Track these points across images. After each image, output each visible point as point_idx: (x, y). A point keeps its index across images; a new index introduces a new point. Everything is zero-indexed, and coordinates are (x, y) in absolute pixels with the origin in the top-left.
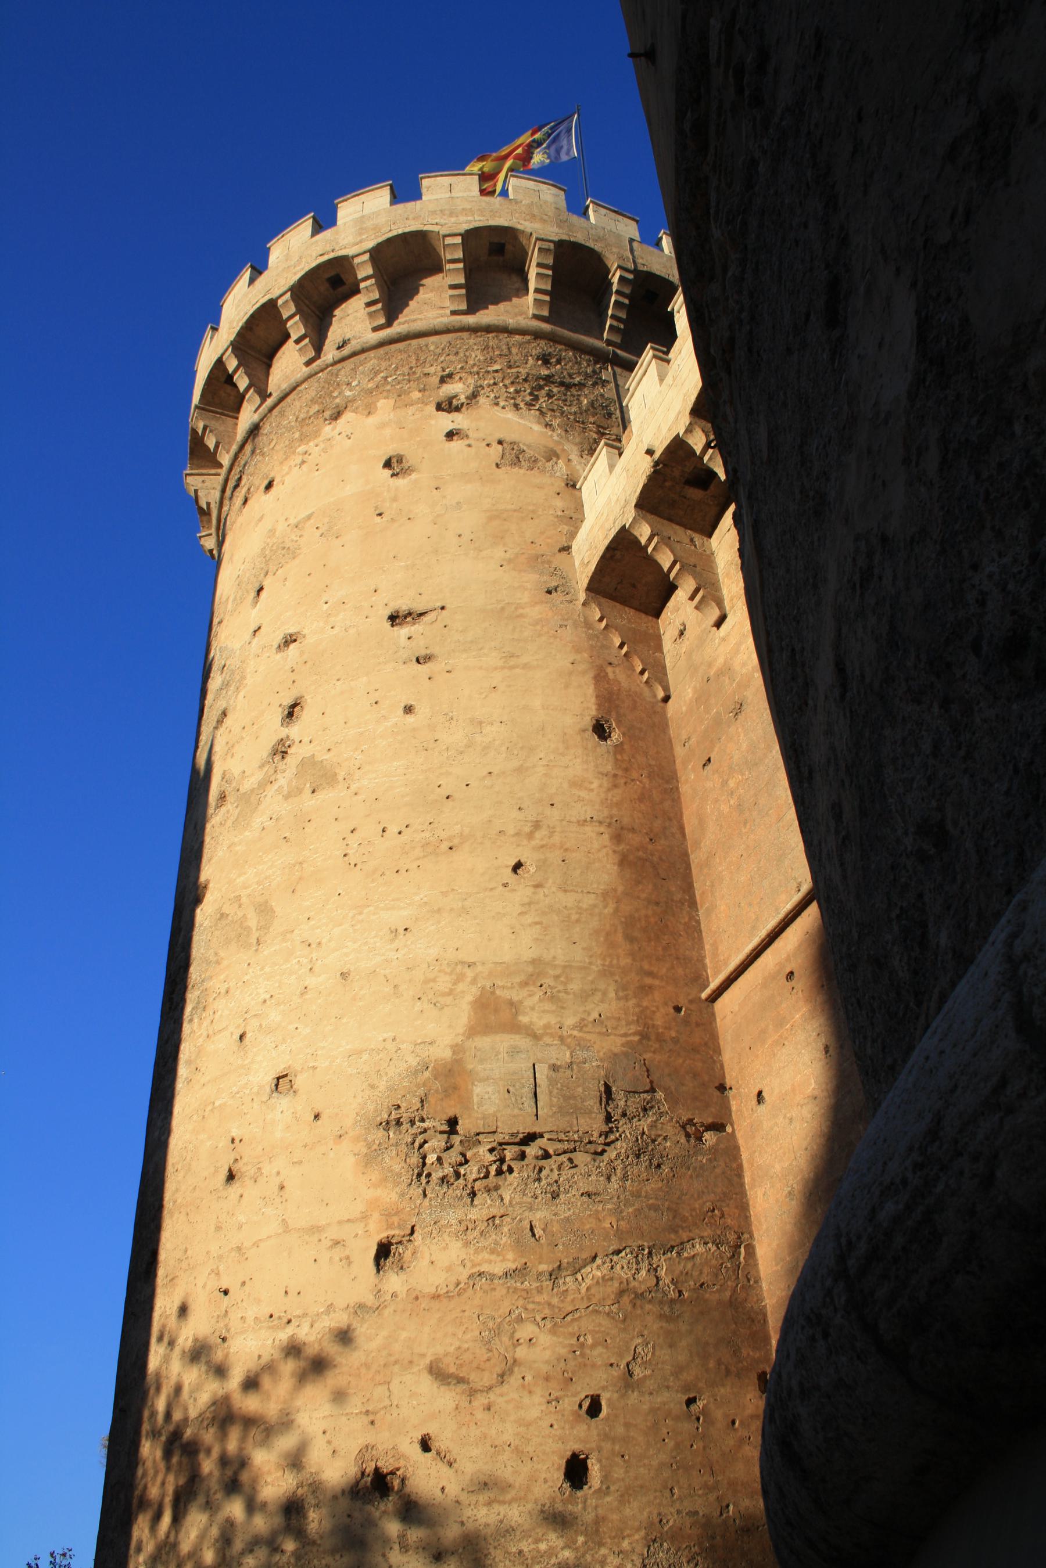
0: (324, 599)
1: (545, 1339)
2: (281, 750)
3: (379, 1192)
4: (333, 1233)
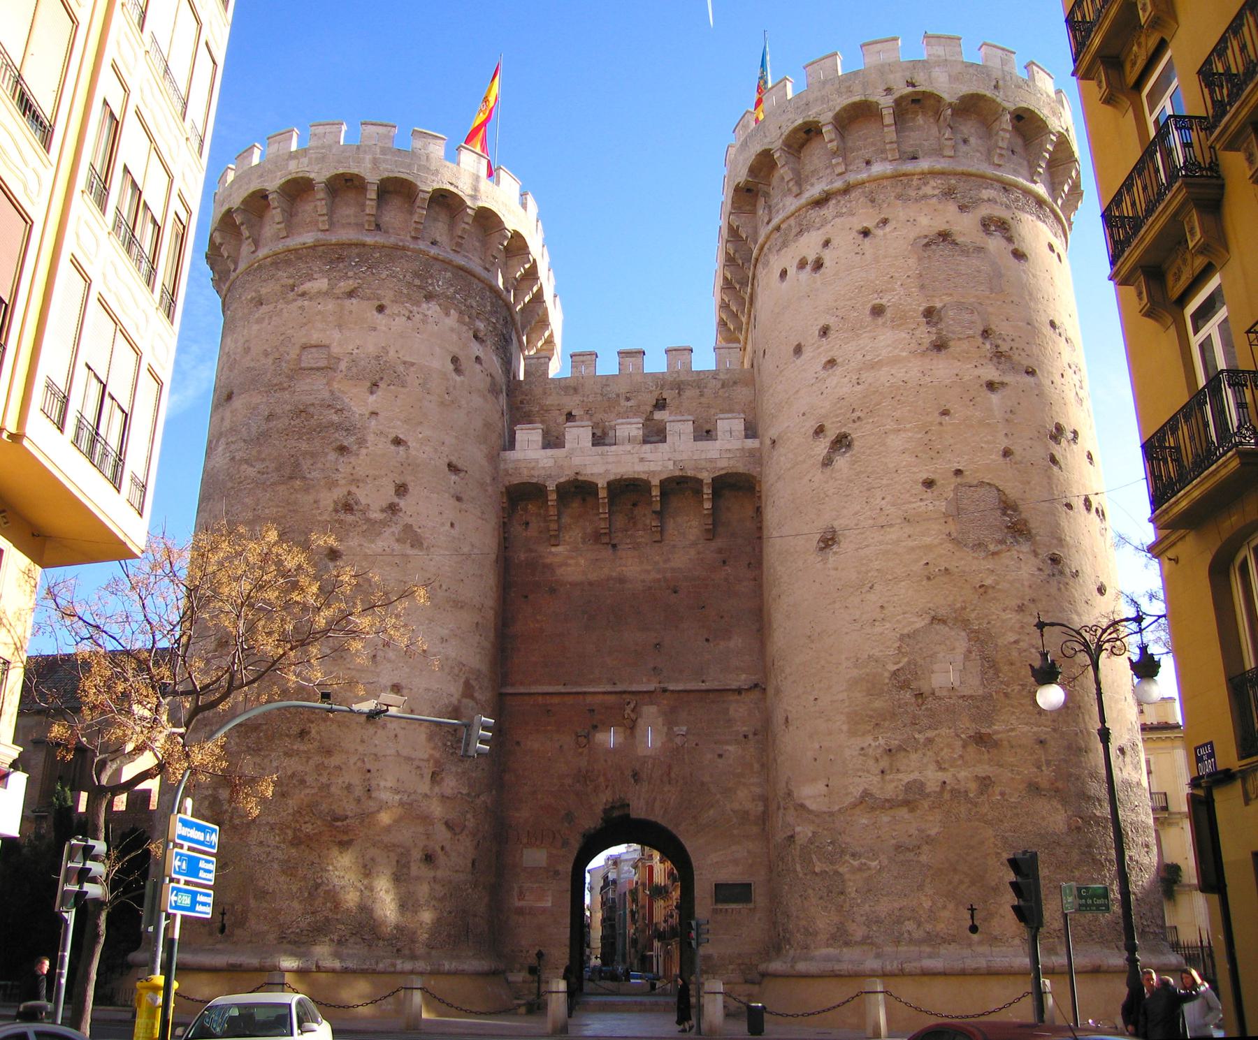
2: (392, 509)
4: (416, 763)
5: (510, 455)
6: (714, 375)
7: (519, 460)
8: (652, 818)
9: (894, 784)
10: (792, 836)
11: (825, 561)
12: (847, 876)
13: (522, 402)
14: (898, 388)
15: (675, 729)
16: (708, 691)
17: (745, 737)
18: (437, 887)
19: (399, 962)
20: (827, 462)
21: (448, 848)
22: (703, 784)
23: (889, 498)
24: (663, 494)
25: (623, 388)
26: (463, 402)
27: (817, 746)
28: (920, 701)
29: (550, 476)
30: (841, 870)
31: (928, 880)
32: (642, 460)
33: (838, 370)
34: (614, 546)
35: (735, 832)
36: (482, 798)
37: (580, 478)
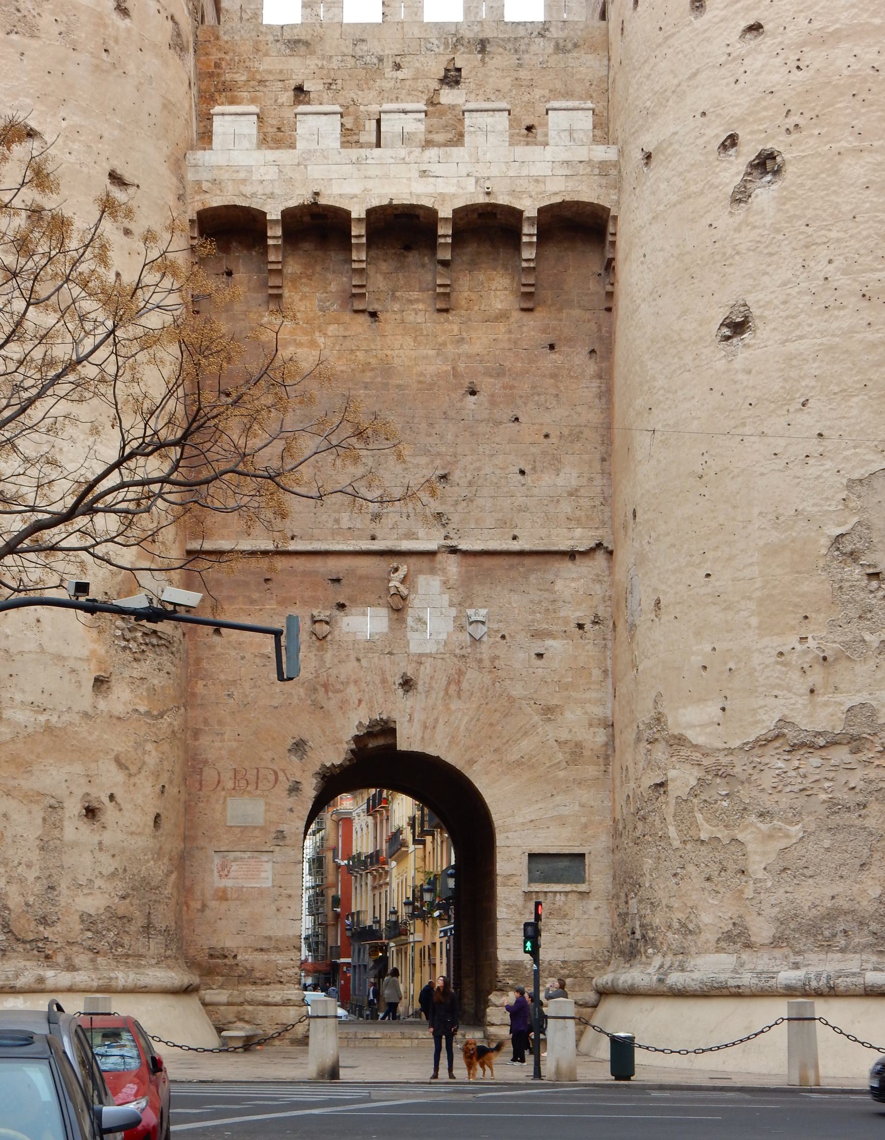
0: (62, 114)
1: (154, 753)
3: (95, 646)
4: (71, 663)
5: (203, 157)
6: (543, 30)
7: (220, 167)
8: (432, 751)
9: (830, 710)
10: (662, 785)
11: (731, 357)
12: (750, 847)
13: (217, 65)
14: (865, 80)
15: (470, 612)
16: (521, 553)
17: (580, 626)
18: (104, 857)
19: (49, 973)
20: (741, 196)
21: (118, 798)
22: (511, 699)
23: (839, 262)
24: (457, 235)
25: (390, 48)
26: (131, 67)
27: (708, 648)
28: (874, 584)
29: (272, 196)
30: (740, 837)
31: (877, 856)
32: (424, 173)
33: (765, 43)
34: (374, 315)
35: (561, 774)
36: (167, 719)
37: (322, 201)
